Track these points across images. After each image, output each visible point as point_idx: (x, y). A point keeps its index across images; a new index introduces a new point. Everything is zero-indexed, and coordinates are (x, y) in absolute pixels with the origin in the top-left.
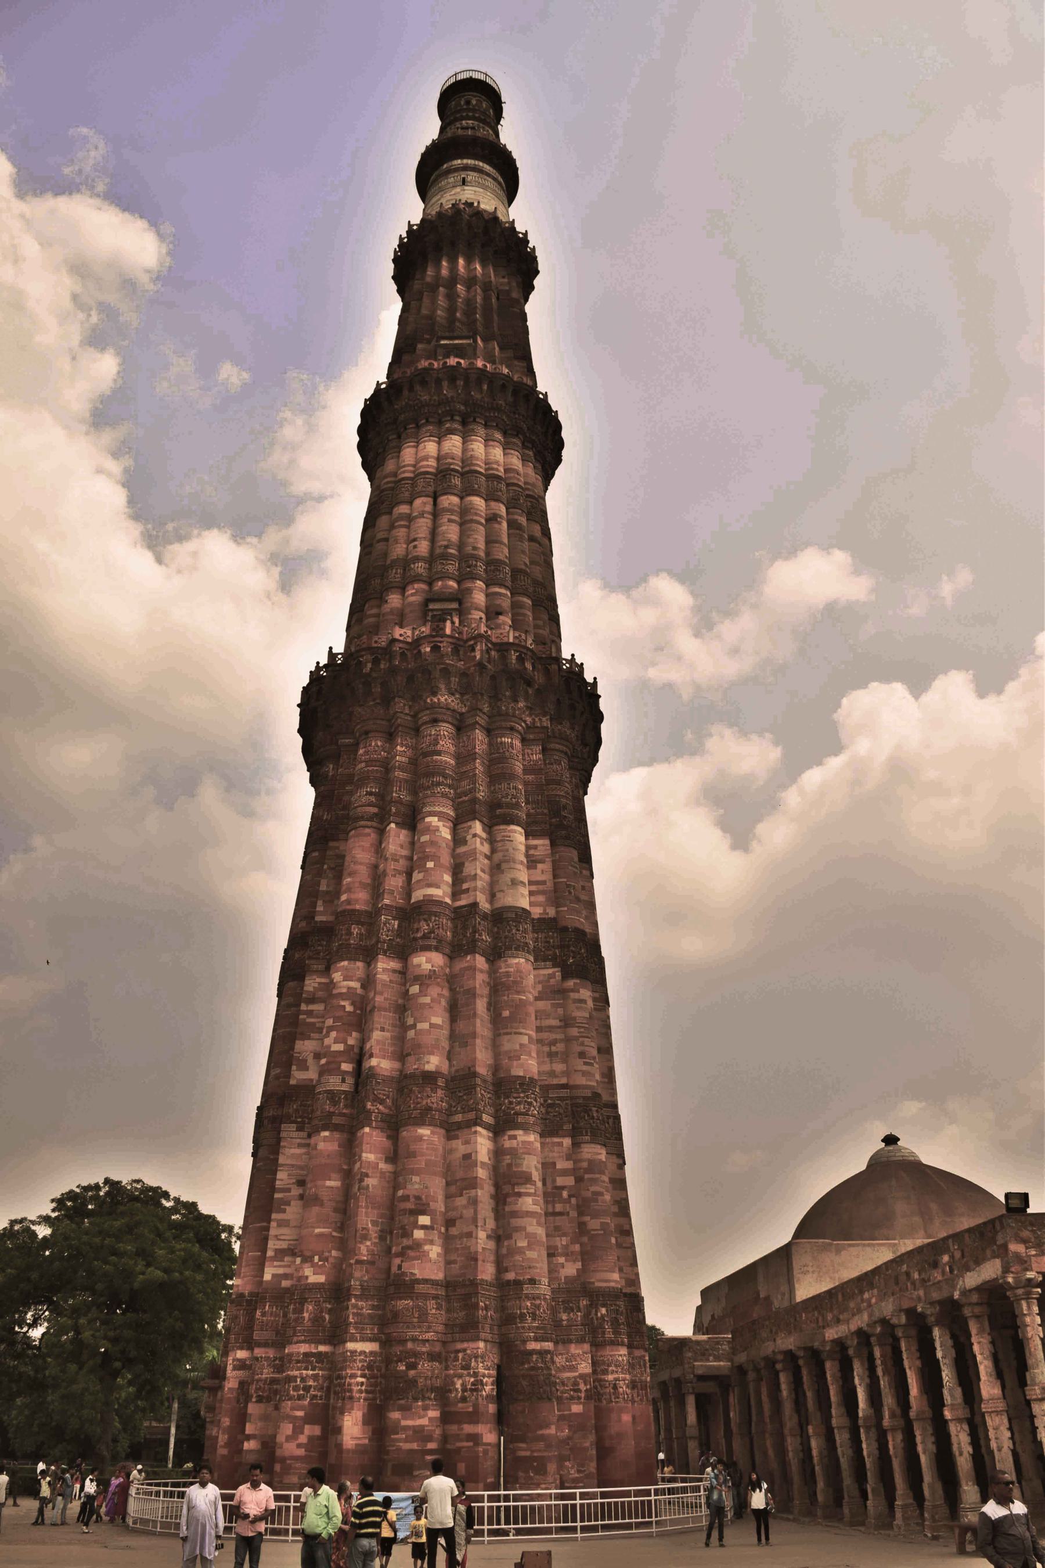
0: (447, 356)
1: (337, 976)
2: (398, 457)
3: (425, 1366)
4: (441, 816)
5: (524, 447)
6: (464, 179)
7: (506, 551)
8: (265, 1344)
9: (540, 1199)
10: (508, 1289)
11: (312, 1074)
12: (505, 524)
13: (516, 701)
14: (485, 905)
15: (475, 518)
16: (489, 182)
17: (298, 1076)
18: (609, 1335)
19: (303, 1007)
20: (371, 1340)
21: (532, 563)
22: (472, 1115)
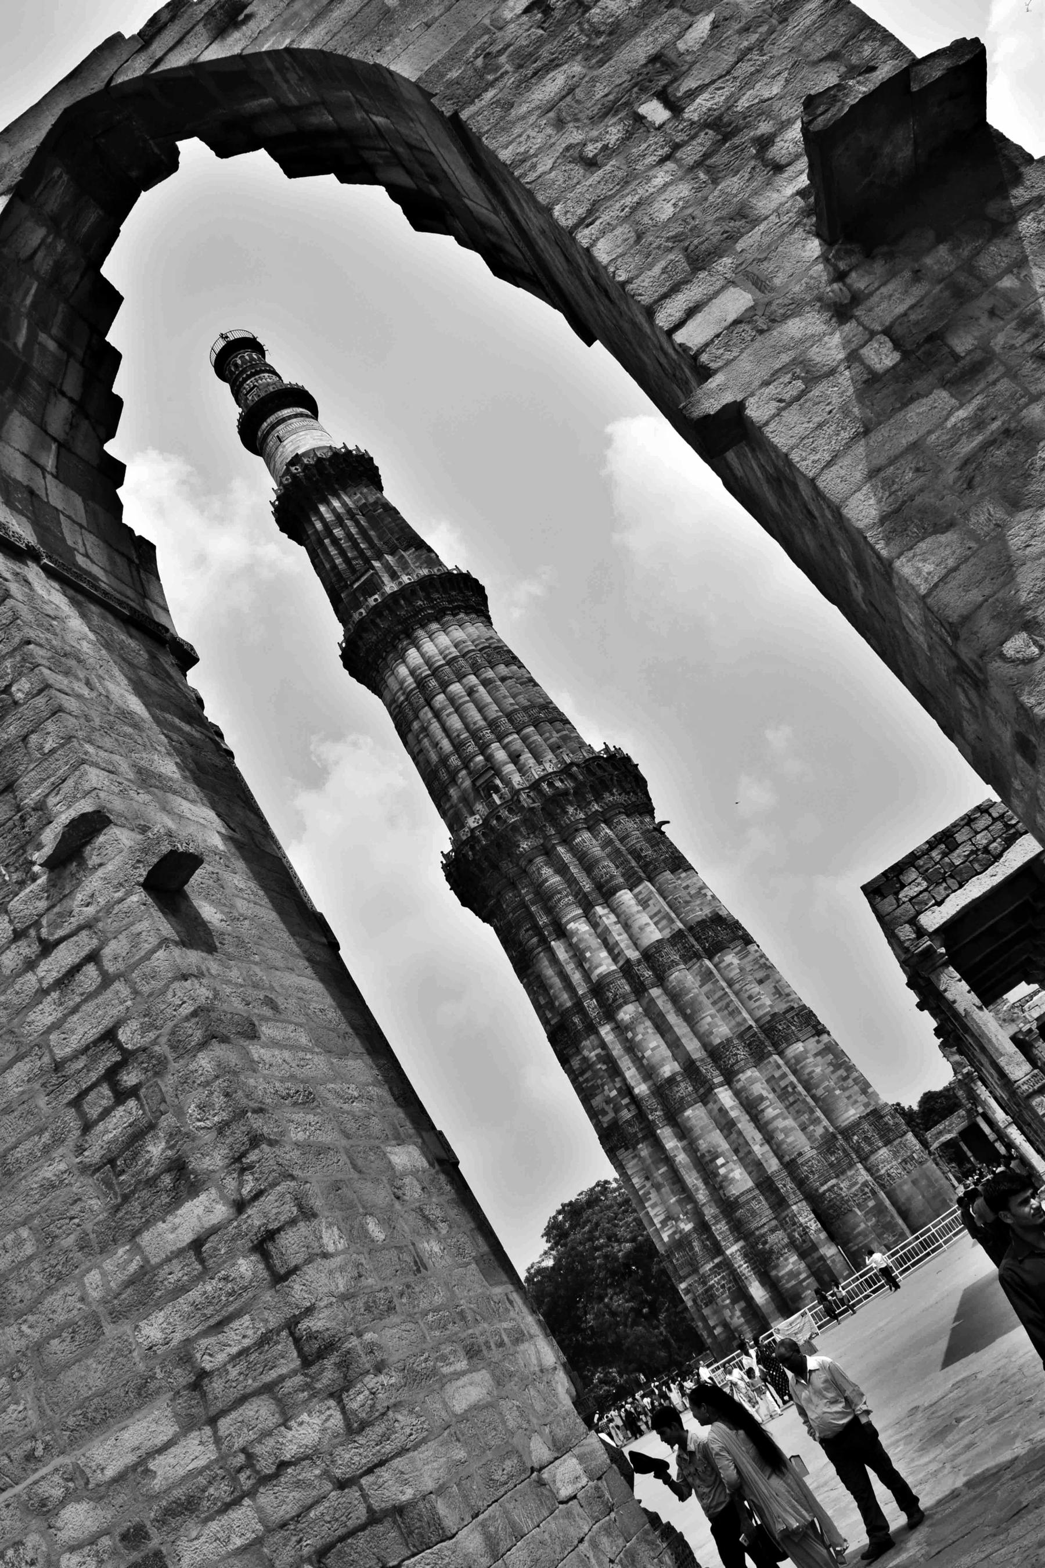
1: (586, 1053)
3: (772, 1239)
4: (574, 919)
5: (454, 615)
7: (495, 707)
8: (689, 1275)
9: (779, 1104)
10: (790, 1166)
11: (611, 1115)
12: (481, 689)
14: (633, 955)
16: (296, 423)
17: (606, 1120)
18: (867, 1149)
20: (736, 1241)
21: (514, 697)
22: (707, 1086)
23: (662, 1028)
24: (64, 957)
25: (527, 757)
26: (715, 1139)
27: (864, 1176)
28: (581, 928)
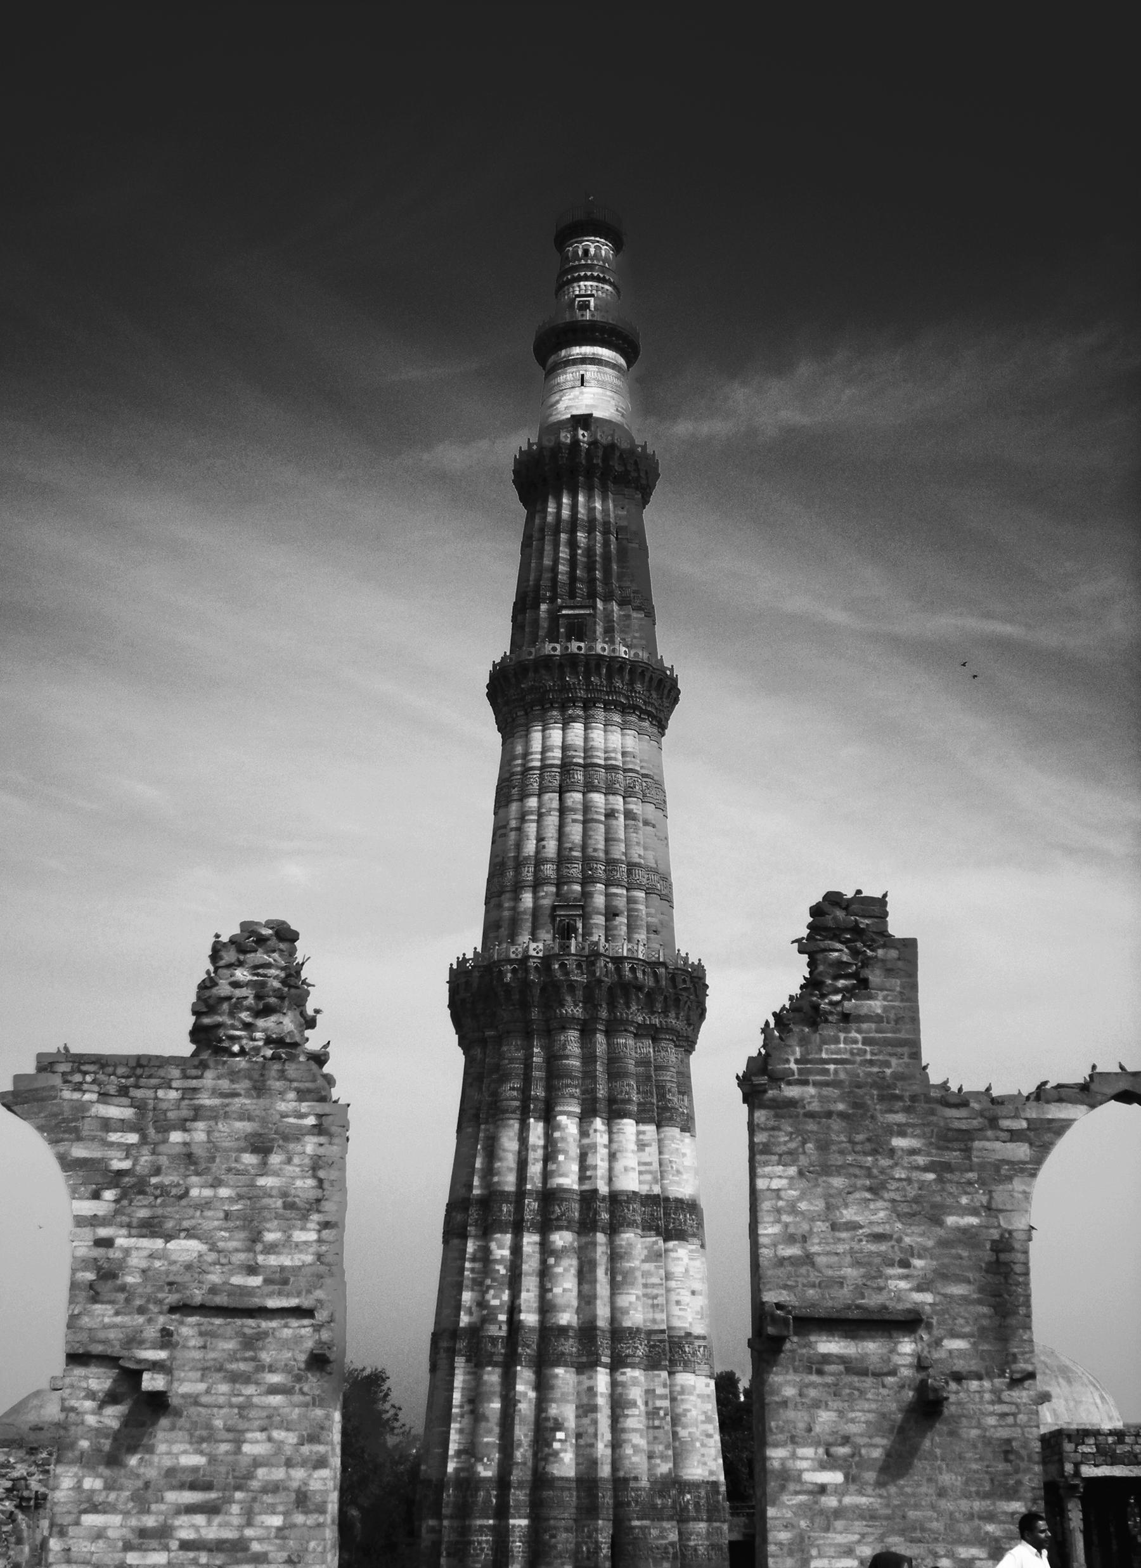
0: (569, 640)
1: (493, 1246)
2: (527, 736)
4: (568, 1114)
6: (583, 376)
9: (643, 1419)
10: (620, 1483)
12: (622, 818)
13: (629, 1008)
14: (603, 1189)
15: (596, 817)
16: (609, 375)
17: (464, 1320)
18: (693, 1514)
19: (467, 1265)
21: (645, 849)
23: (585, 1274)
24: (1005, 1408)
25: (622, 920)
26: (566, 1411)
27: (673, 1536)
28: (569, 1125)
